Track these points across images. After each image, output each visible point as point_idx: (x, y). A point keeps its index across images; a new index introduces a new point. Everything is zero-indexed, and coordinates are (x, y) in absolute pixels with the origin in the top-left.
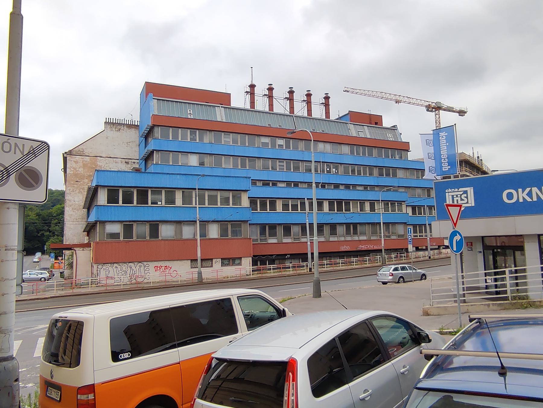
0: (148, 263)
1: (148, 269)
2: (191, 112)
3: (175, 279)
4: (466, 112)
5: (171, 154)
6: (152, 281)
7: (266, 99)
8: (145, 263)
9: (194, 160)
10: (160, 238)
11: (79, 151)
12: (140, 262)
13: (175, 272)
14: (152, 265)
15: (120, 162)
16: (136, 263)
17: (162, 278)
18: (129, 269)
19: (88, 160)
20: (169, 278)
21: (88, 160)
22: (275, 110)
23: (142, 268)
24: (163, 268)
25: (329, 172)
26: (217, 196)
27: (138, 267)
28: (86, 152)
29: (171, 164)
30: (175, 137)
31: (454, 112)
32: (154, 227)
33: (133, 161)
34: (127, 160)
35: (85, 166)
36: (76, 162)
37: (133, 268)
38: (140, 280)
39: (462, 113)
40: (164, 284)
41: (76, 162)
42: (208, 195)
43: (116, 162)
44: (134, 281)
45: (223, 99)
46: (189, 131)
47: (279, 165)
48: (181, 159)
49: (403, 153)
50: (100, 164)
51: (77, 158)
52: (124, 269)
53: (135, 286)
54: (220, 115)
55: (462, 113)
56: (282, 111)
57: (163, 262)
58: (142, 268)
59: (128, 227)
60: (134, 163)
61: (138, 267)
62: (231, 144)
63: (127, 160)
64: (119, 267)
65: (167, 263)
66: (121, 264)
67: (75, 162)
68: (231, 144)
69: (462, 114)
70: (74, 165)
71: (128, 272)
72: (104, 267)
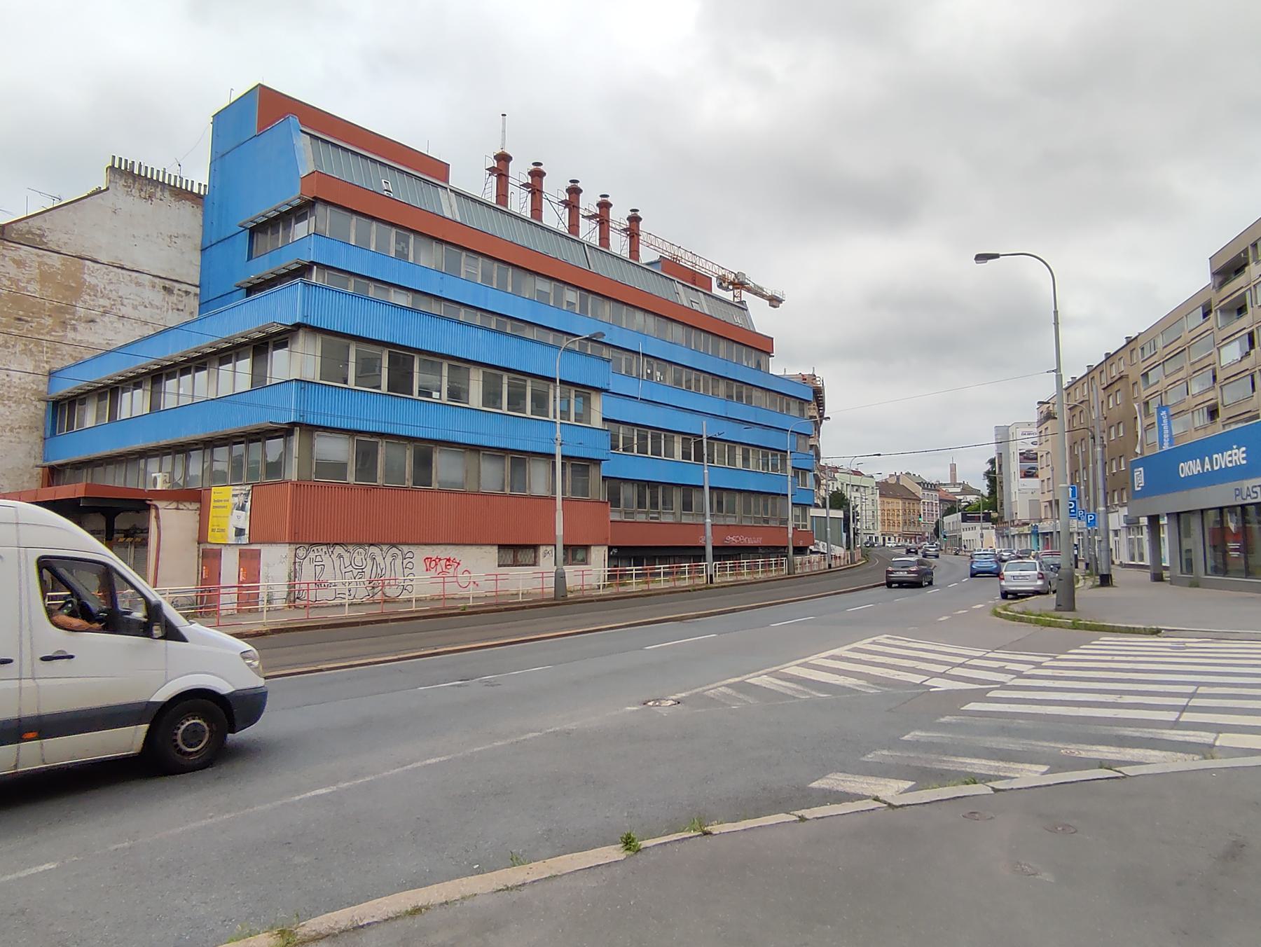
0: (412, 548)
1: (410, 565)
2: (387, 184)
3: (464, 593)
4: (781, 301)
6: (413, 596)
8: (405, 549)
10: (435, 486)
11: (29, 232)
12: (394, 545)
13: (466, 574)
15: (147, 283)
16: (385, 548)
17: (437, 590)
18: (370, 562)
19: (58, 265)
20: (452, 589)
21: (58, 265)
23: (398, 561)
24: (443, 562)
25: (650, 376)
27: (389, 559)
28: (53, 240)
31: (763, 296)
33: (184, 287)
34: (168, 284)
35: (45, 277)
36: (20, 264)
37: (379, 559)
38: (391, 592)
39: (775, 301)
40: (439, 605)
41: (20, 264)
43: (138, 284)
44: (378, 597)
49: (764, 356)
50: (93, 281)
51: (22, 253)
53: (376, 610)
55: (775, 301)
57: (442, 548)
58: (398, 561)
60: (187, 293)
63: (168, 284)
64: (346, 555)
66: (350, 548)
67: (14, 261)
69: (775, 303)
70: (13, 271)
71: (367, 570)
72: (312, 555)
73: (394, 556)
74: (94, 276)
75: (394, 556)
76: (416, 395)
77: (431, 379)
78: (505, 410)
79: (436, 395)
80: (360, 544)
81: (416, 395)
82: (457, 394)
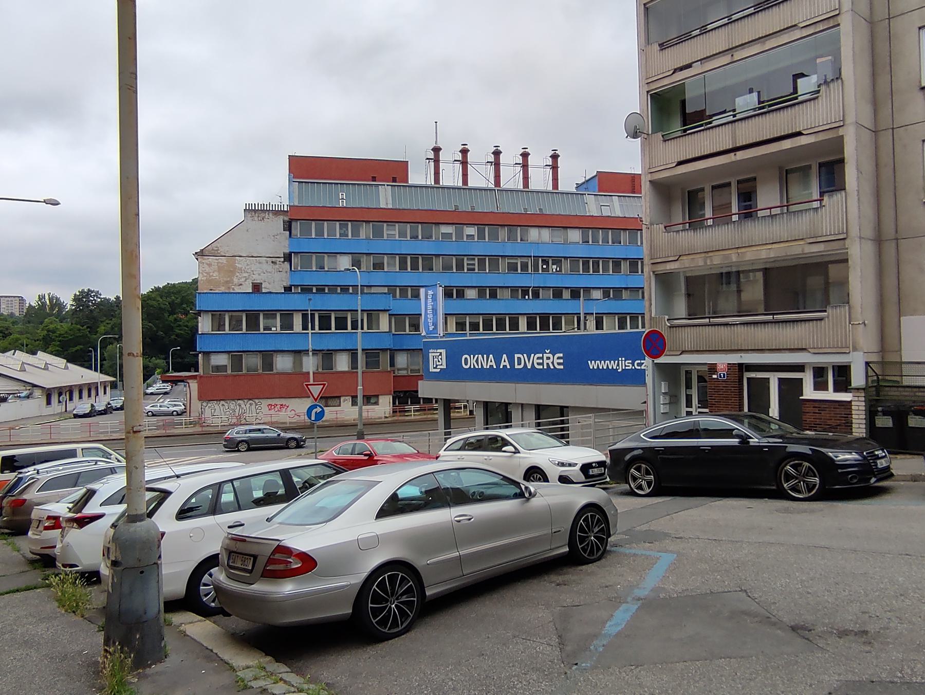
5: (314, 256)
7: (458, 166)
8: (257, 401)
9: (344, 262)
10: (275, 371)
14: (265, 403)
22: (470, 184)
23: (253, 406)
26: (346, 318)
27: (248, 405)
29: (314, 269)
30: (320, 233)
32: (268, 357)
37: (243, 406)
42: (336, 318)
45: (394, 172)
46: (338, 223)
47: (474, 265)
48: (327, 262)
52: (232, 407)
54: (385, 197)
56: (482, 184)
58: (253, 406)
59: (237, 358)
61: (248, 405)
62: (397, 238)
65: (283, 401)
68: (397, 238)
71: (237, 411)
73: (251, 404)
74: (240, 263)
75: (251, 404)
76: (262, 331)
77: (270, 322)
78: (333, 330)
79: (273, 329)
80: (233, 400)
81: (262, 331)
82: (287, 324)
